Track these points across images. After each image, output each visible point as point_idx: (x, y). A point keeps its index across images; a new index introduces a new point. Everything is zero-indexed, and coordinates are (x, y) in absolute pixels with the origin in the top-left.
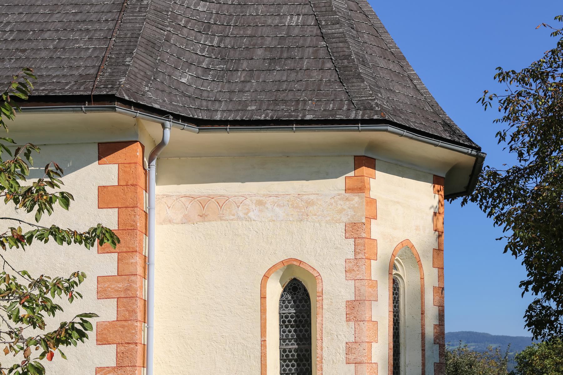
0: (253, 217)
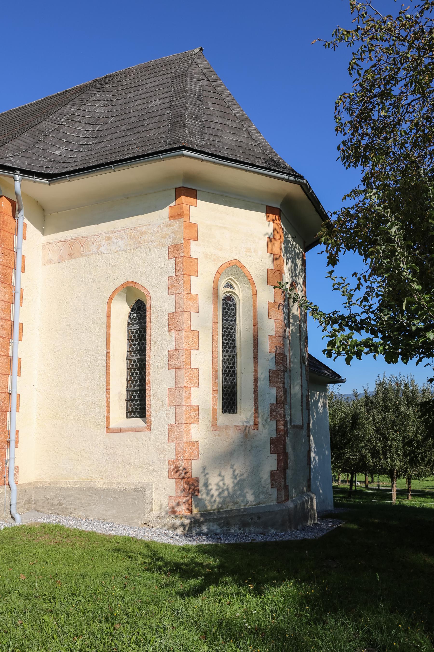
0: (103, 251)
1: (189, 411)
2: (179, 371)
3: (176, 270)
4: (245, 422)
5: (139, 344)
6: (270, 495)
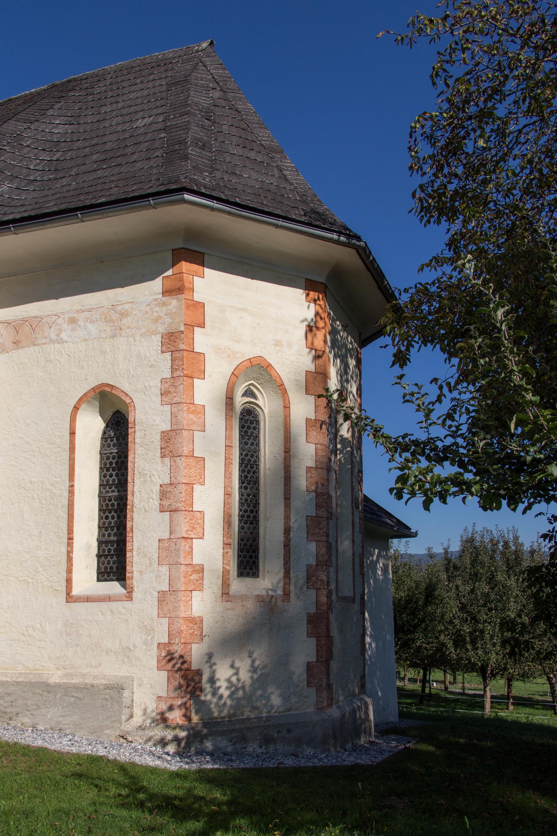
0: (65, 338)
1: (189, 573)
2: (175, 515)
3: (173, 370)
4: (270, 590)
5: (117, 475)
6: (306, 697)
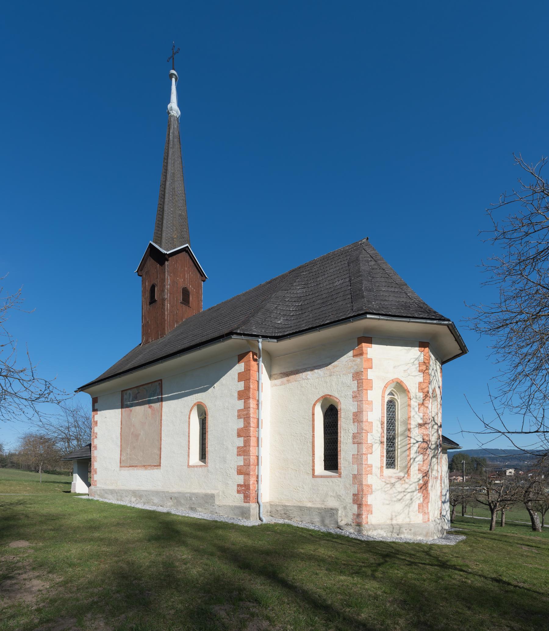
2: (360, 445)
